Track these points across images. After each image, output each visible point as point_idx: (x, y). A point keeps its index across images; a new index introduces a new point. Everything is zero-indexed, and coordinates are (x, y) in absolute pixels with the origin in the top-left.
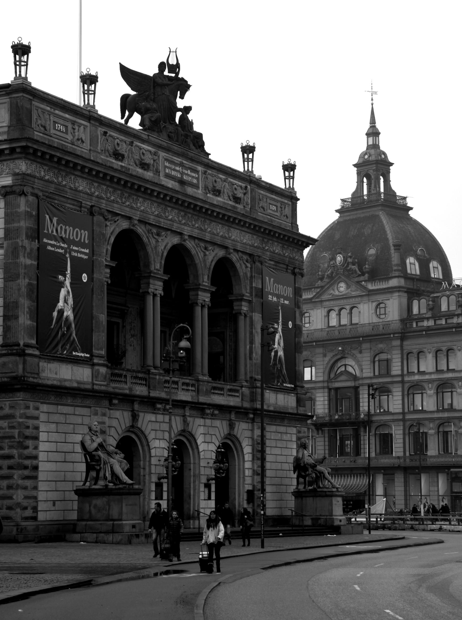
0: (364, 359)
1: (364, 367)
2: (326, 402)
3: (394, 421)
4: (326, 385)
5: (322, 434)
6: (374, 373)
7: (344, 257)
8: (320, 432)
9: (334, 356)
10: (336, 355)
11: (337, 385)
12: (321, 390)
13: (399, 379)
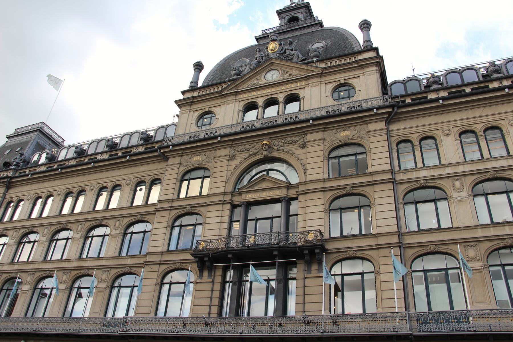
0: (309, 155)
1: (308, 167)
2: (226, 225)
3: (378, 248)
4: (228, 198)
5: (209, 276)
6: (329, 175)
7: (280, 45)
8: (206, 273)
9: (250, 155)
10: (255, 154)
11: (250, 197)
12: (220, 207)
13: (389, 176)
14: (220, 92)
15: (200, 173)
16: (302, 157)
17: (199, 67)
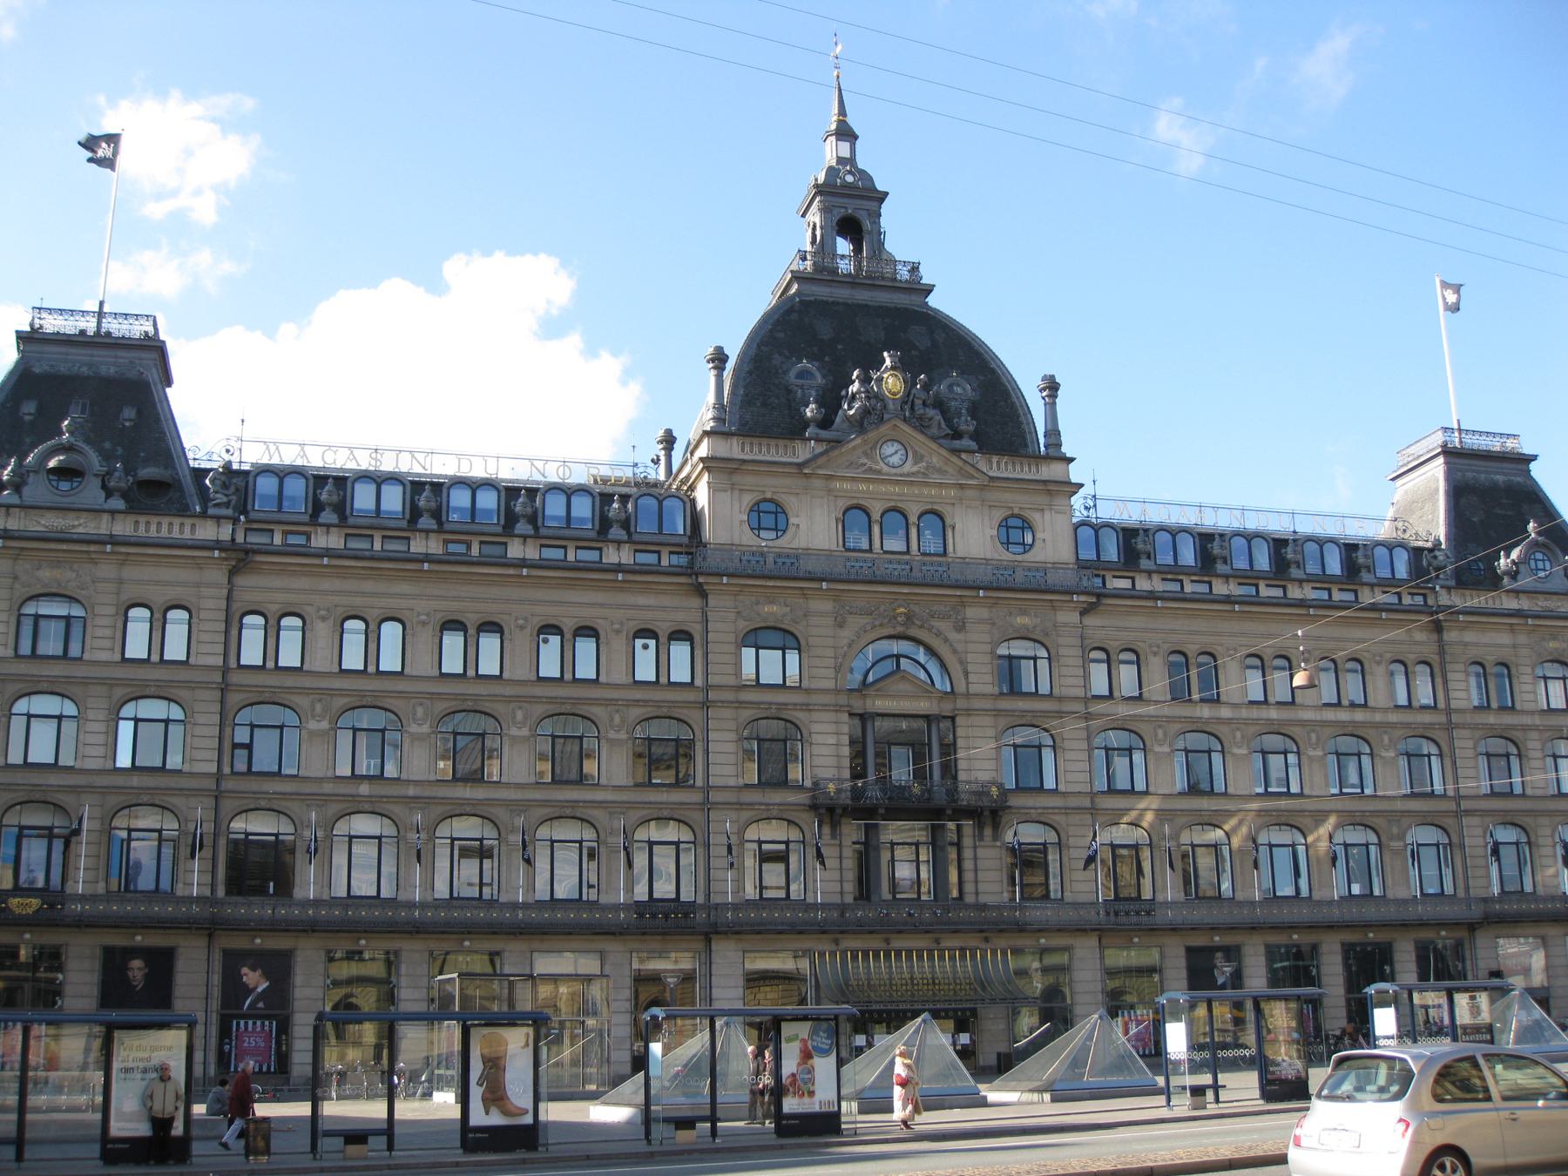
0: (971, 647)
4: (843, 699)
12: (831, 716)
14: (800, 466)
15: (777, 638)
16: (959, 647)
17: (719, 359)
